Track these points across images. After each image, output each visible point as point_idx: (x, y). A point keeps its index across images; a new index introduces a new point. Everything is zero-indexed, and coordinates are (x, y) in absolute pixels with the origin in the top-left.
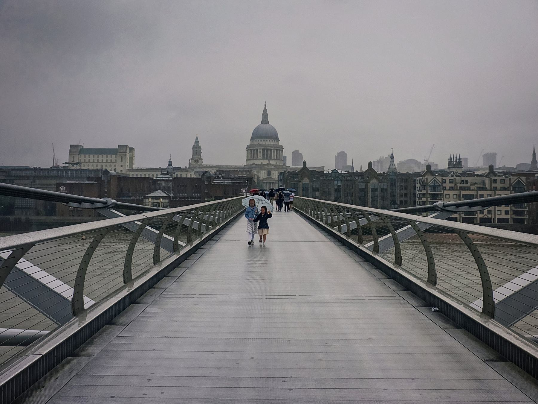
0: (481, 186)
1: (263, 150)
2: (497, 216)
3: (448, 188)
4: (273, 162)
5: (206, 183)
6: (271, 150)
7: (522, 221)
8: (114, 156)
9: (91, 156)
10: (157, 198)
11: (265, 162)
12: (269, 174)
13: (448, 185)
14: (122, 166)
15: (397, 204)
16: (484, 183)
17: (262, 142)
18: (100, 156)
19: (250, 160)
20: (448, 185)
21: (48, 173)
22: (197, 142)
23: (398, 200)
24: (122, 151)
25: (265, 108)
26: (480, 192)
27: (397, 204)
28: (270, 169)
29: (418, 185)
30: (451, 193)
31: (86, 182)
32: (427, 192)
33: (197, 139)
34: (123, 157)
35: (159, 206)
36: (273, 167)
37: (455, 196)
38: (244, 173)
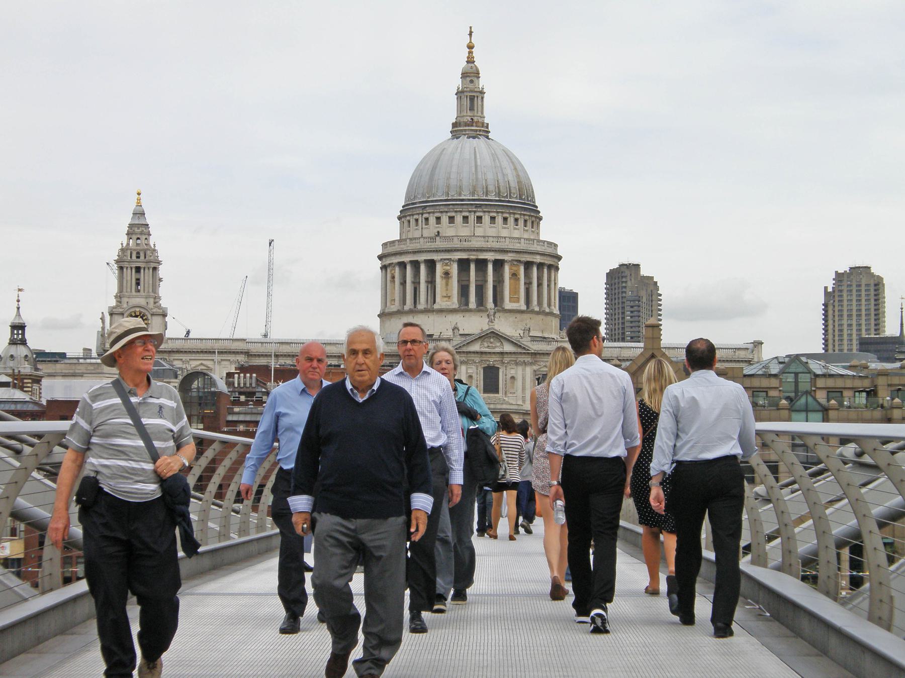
1: (464, 264)
4: (505, 326)
11: (474, 324)
19: (400, 313)
22: (138, 229)
25: (470, 60)
28: (492, 361)
33: (139, 213)
36: (508, 348)
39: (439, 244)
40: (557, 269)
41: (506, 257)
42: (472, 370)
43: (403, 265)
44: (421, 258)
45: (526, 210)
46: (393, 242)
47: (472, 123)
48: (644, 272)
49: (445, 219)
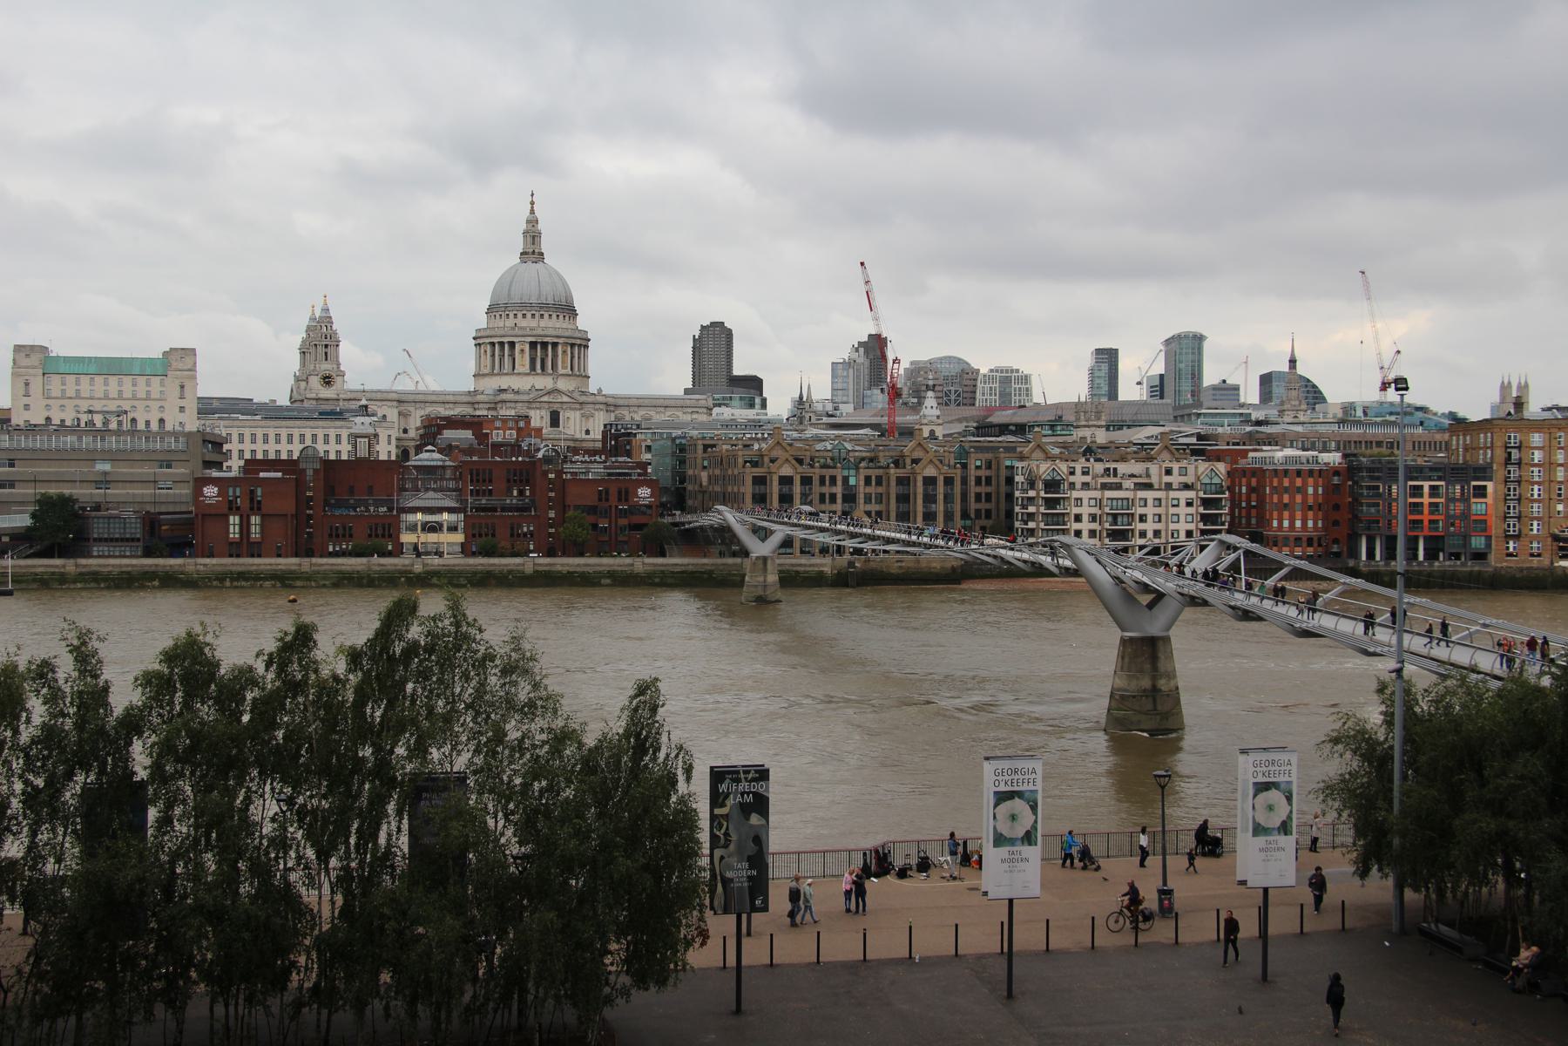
1: (533, 345)
3: (1078, 486)
4: (562, 384)
5: (552, 476)
6: (555, 345)
8: (156, 381)
9: (85, 380)
12: (555, 420)
13: (1079, 479)
14: (182, 409)
16: (1148, 476)
18: (113, 380)
19: (492, 374)
20: (1079, 479)
21: (50, 440)
22: (326, 320)
23: (973, 506)
24: (181, 366)
25: (532, 211)
26: (1141, 494)
28: (555, 407)
29: (1019, 479)
30: (1085, 495)
31: (262, 475)
37: (1093, 502)
38: (511, 424)
39: (517, 331)
40: (586, 347)
43: (493, 344)
44: (506, 340)
49: (520, 315)
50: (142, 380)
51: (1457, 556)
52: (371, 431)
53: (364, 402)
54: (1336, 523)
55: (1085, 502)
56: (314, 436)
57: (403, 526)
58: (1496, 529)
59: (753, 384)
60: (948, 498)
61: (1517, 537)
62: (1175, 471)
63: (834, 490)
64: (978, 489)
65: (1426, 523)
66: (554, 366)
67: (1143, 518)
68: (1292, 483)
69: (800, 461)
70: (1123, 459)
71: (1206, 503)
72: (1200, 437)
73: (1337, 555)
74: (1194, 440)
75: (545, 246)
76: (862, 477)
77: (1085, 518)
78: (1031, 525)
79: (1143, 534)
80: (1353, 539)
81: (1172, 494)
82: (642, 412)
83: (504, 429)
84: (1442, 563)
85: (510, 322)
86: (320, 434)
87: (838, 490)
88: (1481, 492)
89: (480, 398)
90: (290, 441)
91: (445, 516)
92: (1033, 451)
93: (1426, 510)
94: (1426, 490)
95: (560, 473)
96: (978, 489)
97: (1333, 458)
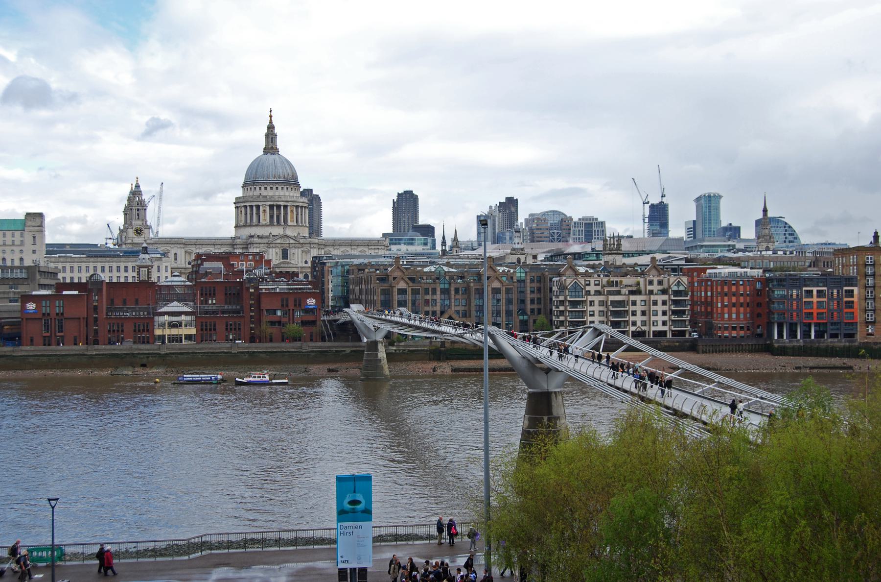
0: (634, 289)
1: (271, 207)
2: (653, 329)
3: (592, 292)
4: (289, 232)
6: (285, 207)
7: (682, 333)
8: (17, 234)
10: (179, 314)
11: (277, 231)
12: (285, 255)
15: (526, 314)
16: (638, 284)
17: (270, 193)
19: (245, 226)
20: (592, 288)
23: (529, 307)
25: (271, 122)
26: (632, 298)
27: (526, 314)
28: (285, 246)
29: (555, 288)
30: (597, 299)
31: (65, 293)
32: (566, 298)
33: (138, 186)
34: (37, 235)
35: (181, 326)
36: (292, 241)
41: (289, 204)
42: (277, 250)
43: (246, 207)
45: (292, 182)
46: (240, 198)
47: (272, 148)
48: (314, 193)
49: (263, 188)
50: (9, 234)
51: (834, 336)
52: (149, 263)
53: (145, 245)
54: (759, 315)
55: (596, 303)
56: (95, 268)
57: (156, 324)
58: (859, 317)
59: (428, 230)
60: (509, 302)
61: (873, 323)
62: (655, 282)
63: (435, 297)
64: (532, 296)
65: (815, 315)
66: (285, 220)
67: (634, 314)
68: (730, 288)
69: (412, 280)
70: (625, 275)
71: (675, 303)
72: (687, 260)
73: (760, 336)
74: (683, 262)
75: (280, 144)
76: (453, 289)
77: (596, 313)
78: (562, 318)
79: (634, 323)
80: (770, 325)
81: (653, 298)
82: (342, 249)
83: (247, 260)
84: (828, 341)
85: (257, 193)
86: (99, 265)
87: (438, 296)
88: (850, 293)
89: (238, 241)
90: (80, 270)
91: (183, 317)
92: (566, 270)
93: (815, 306)
94: (815, 293)
95: (257, 288)
96: (532, 296)
97: (757, 273)
